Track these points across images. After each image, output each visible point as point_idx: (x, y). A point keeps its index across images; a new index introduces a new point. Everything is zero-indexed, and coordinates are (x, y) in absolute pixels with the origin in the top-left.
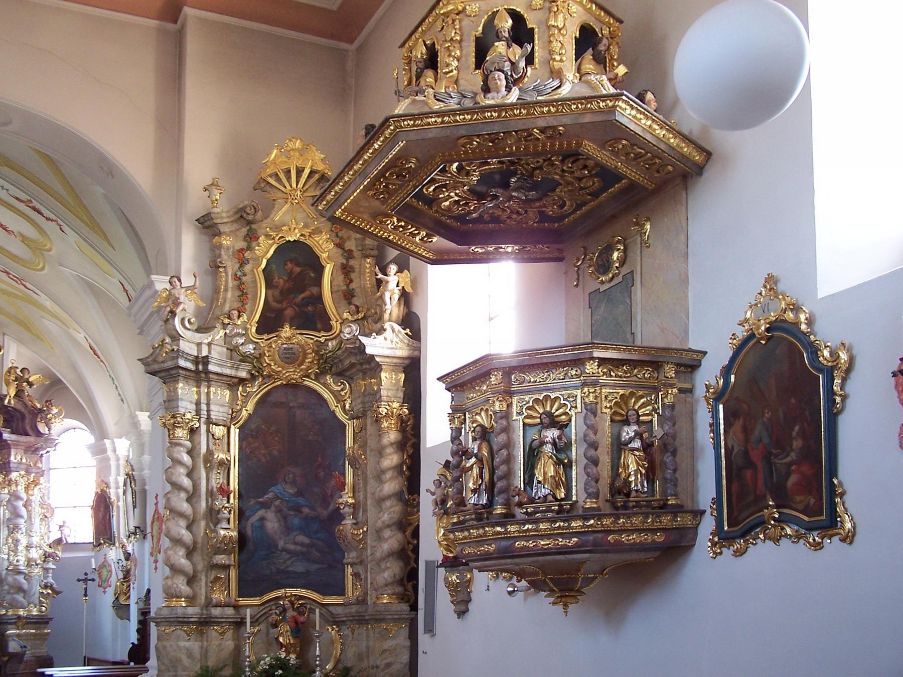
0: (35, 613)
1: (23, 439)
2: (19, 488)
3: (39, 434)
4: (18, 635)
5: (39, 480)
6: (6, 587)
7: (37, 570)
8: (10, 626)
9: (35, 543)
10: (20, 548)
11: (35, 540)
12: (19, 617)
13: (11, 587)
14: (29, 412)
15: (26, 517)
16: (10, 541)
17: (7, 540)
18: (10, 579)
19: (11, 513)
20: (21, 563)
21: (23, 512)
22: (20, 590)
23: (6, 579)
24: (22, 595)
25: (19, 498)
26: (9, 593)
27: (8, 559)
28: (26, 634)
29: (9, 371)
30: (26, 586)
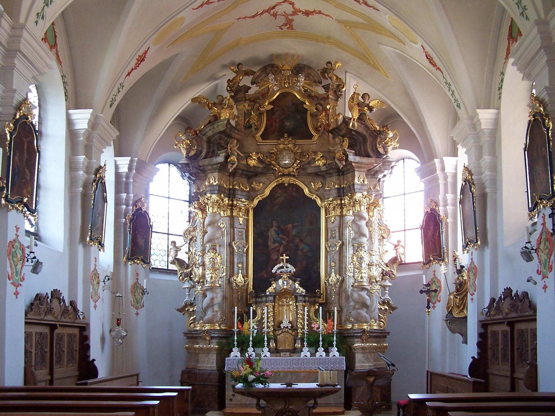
0: (375, 328)
1: (365, 160)
2: (362, 207)
3: (379, 155)
4: (363, 348)
5: (378, 201)
6: (352, 304)
7: (377, 287)
8: (356, 340)
9: (375, 261)
10: (364, 265)
11: (376, 259)
12: (364, 331)
13: (356, 302)
14: (370, 135)
15: (368, 236)
16: (355, 259)
17: (352, 258)
18: (355, 295)
19: (356, 233)
20: (365, 279)
21: (366, 231)
22: (364, 305)
23: (352, 295)
24: (365, 310)
25: (362, 218)
26: (354, 308)
27: (354, 277)
28: (370, 348)
29: (352, 98)
30: (368, 302)
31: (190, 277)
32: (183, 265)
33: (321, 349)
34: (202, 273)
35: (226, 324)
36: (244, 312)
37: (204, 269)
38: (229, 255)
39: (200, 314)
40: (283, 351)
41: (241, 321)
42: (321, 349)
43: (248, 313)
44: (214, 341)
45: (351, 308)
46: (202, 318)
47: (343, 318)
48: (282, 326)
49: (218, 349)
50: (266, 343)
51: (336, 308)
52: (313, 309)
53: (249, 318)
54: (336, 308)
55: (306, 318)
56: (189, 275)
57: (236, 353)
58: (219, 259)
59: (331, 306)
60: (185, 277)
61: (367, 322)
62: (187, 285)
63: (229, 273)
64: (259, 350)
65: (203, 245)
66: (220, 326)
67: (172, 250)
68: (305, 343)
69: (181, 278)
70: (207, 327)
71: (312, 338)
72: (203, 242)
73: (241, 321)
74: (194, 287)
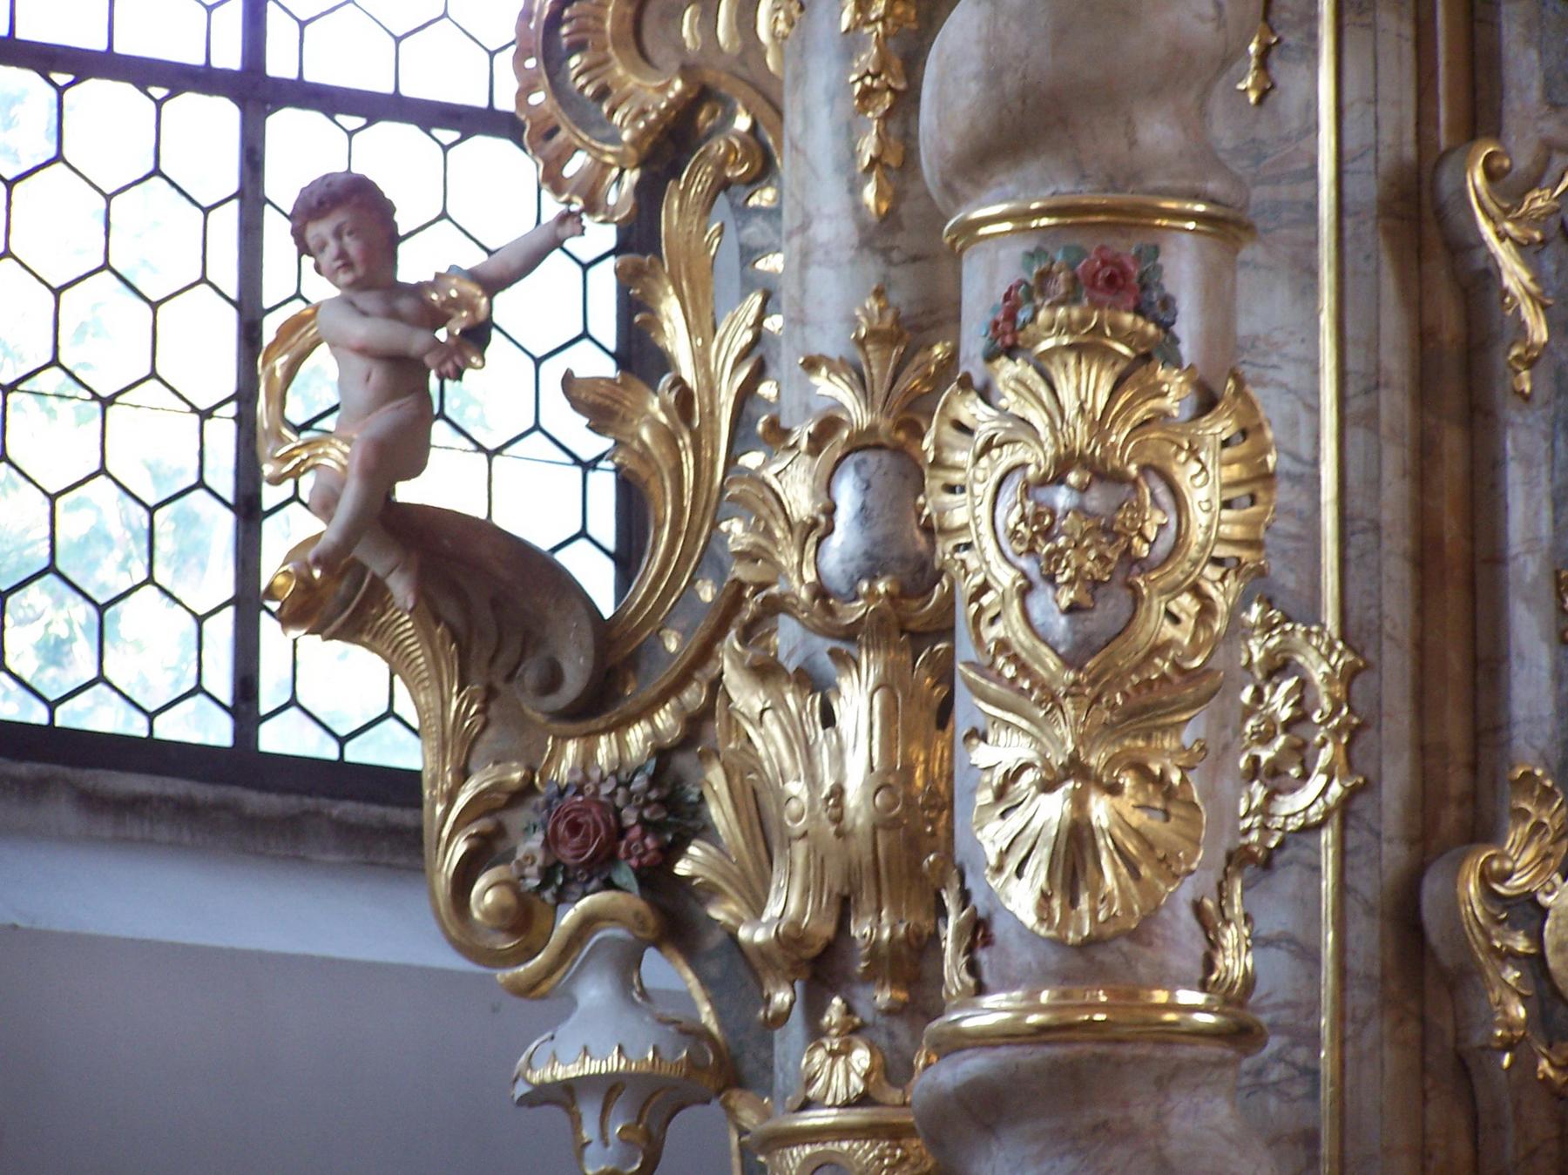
31: (657, 880)
32: (531, 639)
34: (890, 778)
37: (925, 712)
38: (1395, 405)
56: (636, 847)
58: (1202, 485)
60: (560, 880)
62: (591, 1039)
63: (1396, 776)
65: (909, 239)
67: (322, 362)
69: (485, 894)
72: (898, 163)
74: (727, 1067)
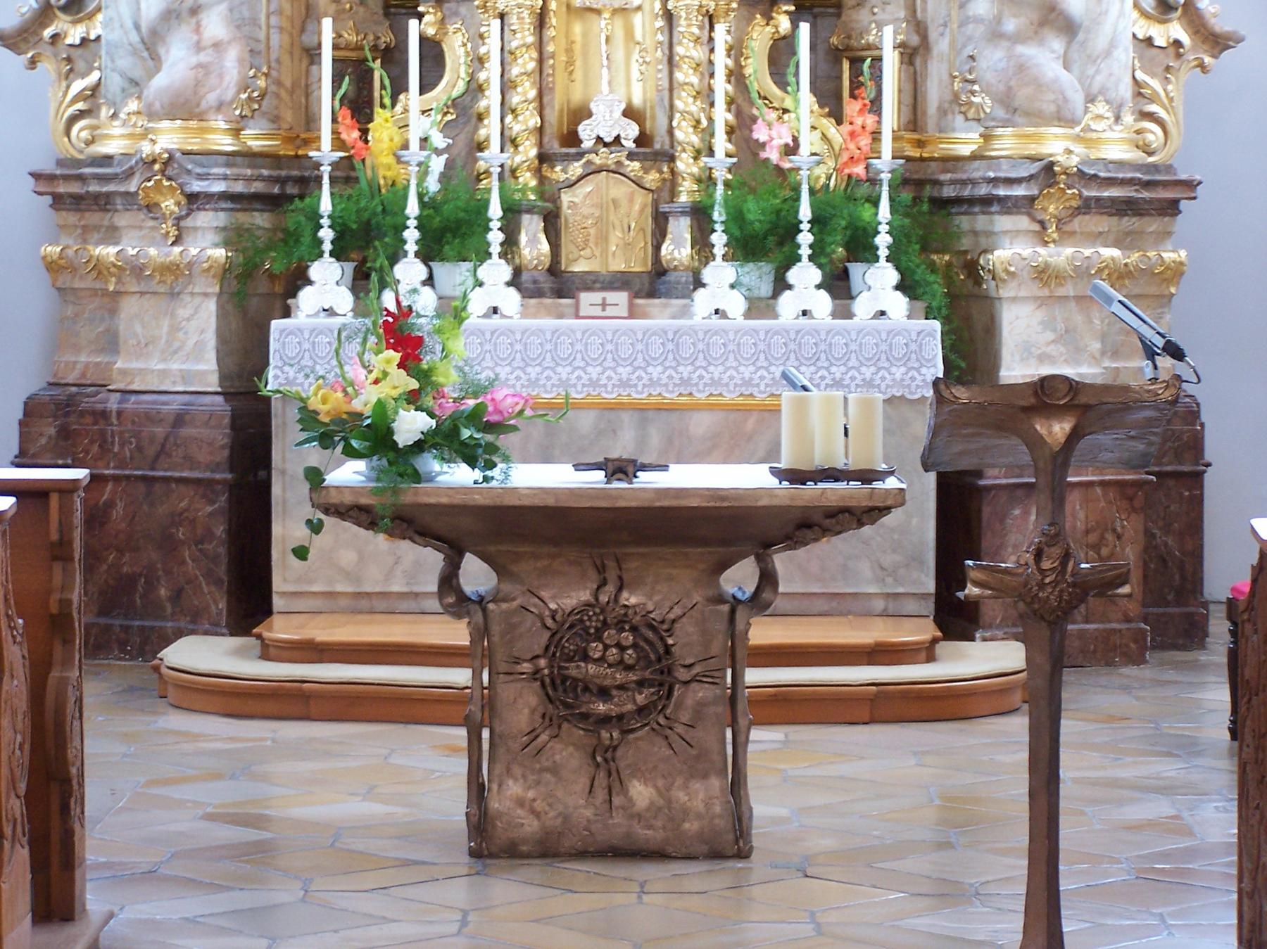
4: (1044, 274)
8: (1004, 222)
12: (1048, 172)
24: (1057, 44)
26: (996, 35)
33: (805, 275)
35: (275, 119)
36: (374, 48)
39: (125, 62)
40: (592, 282)
41: (360, 107)
42: (805, 275)
43: (393, 57)
44: (207, 220)
45: (977, 31)
46: (135, 85)
47: (934, 93)
48: (587, 132)
49: (225, 272)
50: (495, 237)
51: (888, 31)
52: (760, 38)
53: (399, 87)
54: (888, 31)
55: (722, 87)
57: (327, 285)
59: (863, 16)
61: (1063, 118)
64: (453, 275)
66: (236, 132)
68: (719, 239)
70: (169, 137)
71: (754, 211)
73: (360, 107)
